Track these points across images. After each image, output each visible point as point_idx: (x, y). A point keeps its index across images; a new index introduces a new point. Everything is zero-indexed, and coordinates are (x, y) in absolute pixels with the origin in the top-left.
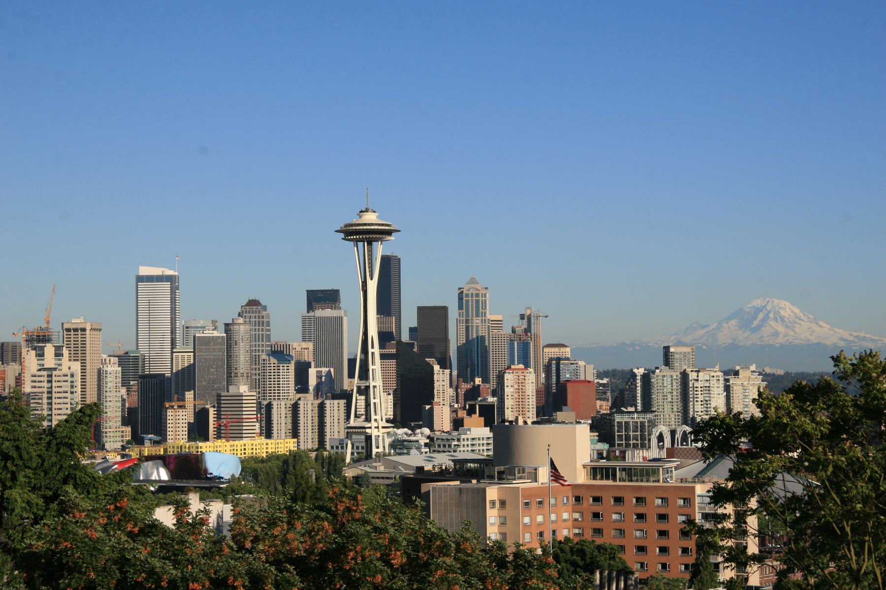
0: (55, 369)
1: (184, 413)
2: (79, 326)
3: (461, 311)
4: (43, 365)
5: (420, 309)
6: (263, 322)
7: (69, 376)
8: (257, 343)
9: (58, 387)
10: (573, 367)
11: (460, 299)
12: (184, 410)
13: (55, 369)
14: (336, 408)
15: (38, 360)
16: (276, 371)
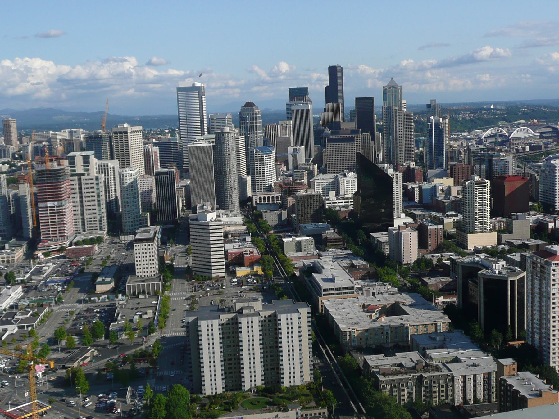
0: (83, 175)
1: (151, 247)
2: (123, 130)
3: (385, 102)
4: (75, 171)
5: (357, 99)
6: (256, 118)
7: (94, 179)
8: (252, 132)
9: (87, 188)
10: (503, 162)
11: (385, 94)
12: (151, 244)
13: (83, 175)
14: (295, 326)
15: (71, 167)
16: (261, 160)
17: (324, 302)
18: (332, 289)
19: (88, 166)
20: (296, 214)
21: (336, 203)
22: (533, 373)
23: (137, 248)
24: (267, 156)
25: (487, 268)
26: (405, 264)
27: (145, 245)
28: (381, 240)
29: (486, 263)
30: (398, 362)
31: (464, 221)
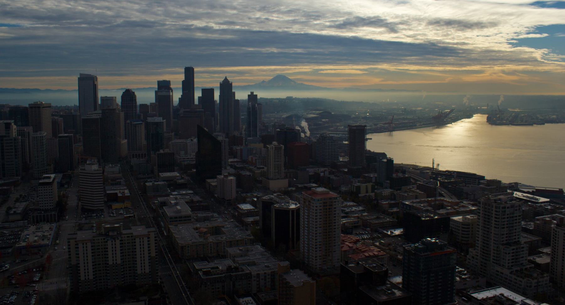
1: (50, 188)
12: (50, 186)
13: (5, 136)
17: (170, 226)
18: (176, 218)
19: (9, 131)
20: (157, 166)
21: (185, 159)
22: (301, 269)
23: (40, 189)
24: (139, 126)
25: (278, 203)
26: (227, 200)
27: (46, 187)
28: (213, 184)
29: (278, 200)
30: (216, 266)
31: (267, 171)
